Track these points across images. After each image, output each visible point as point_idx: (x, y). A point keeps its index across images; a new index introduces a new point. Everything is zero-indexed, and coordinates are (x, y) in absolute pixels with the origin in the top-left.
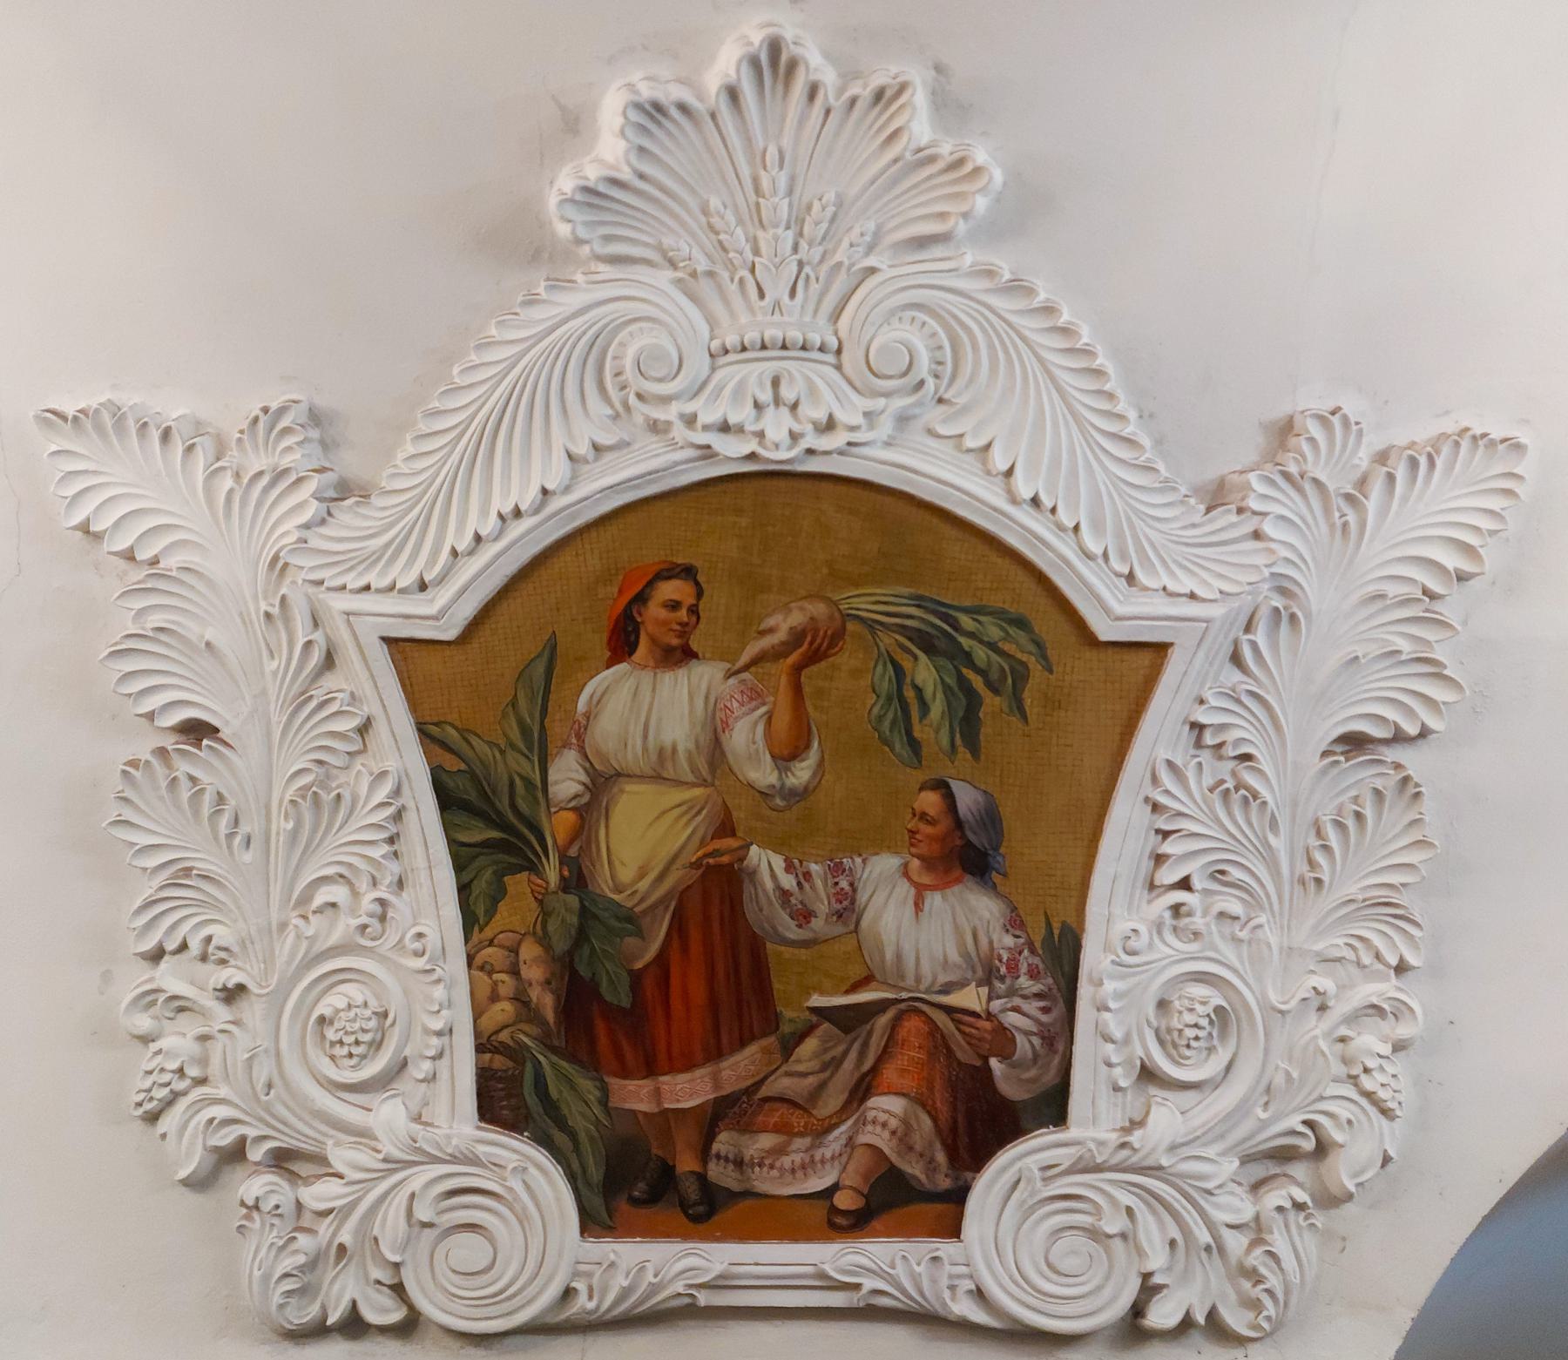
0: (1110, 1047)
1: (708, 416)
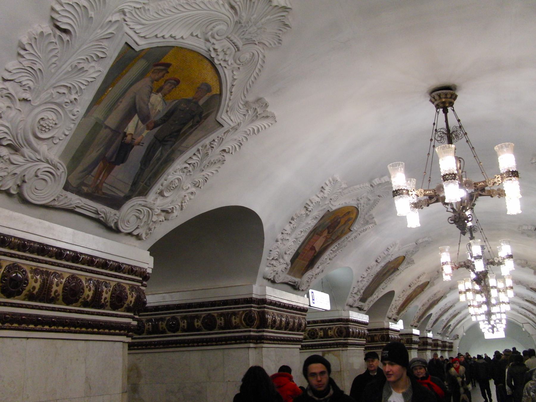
1: (216, 47)
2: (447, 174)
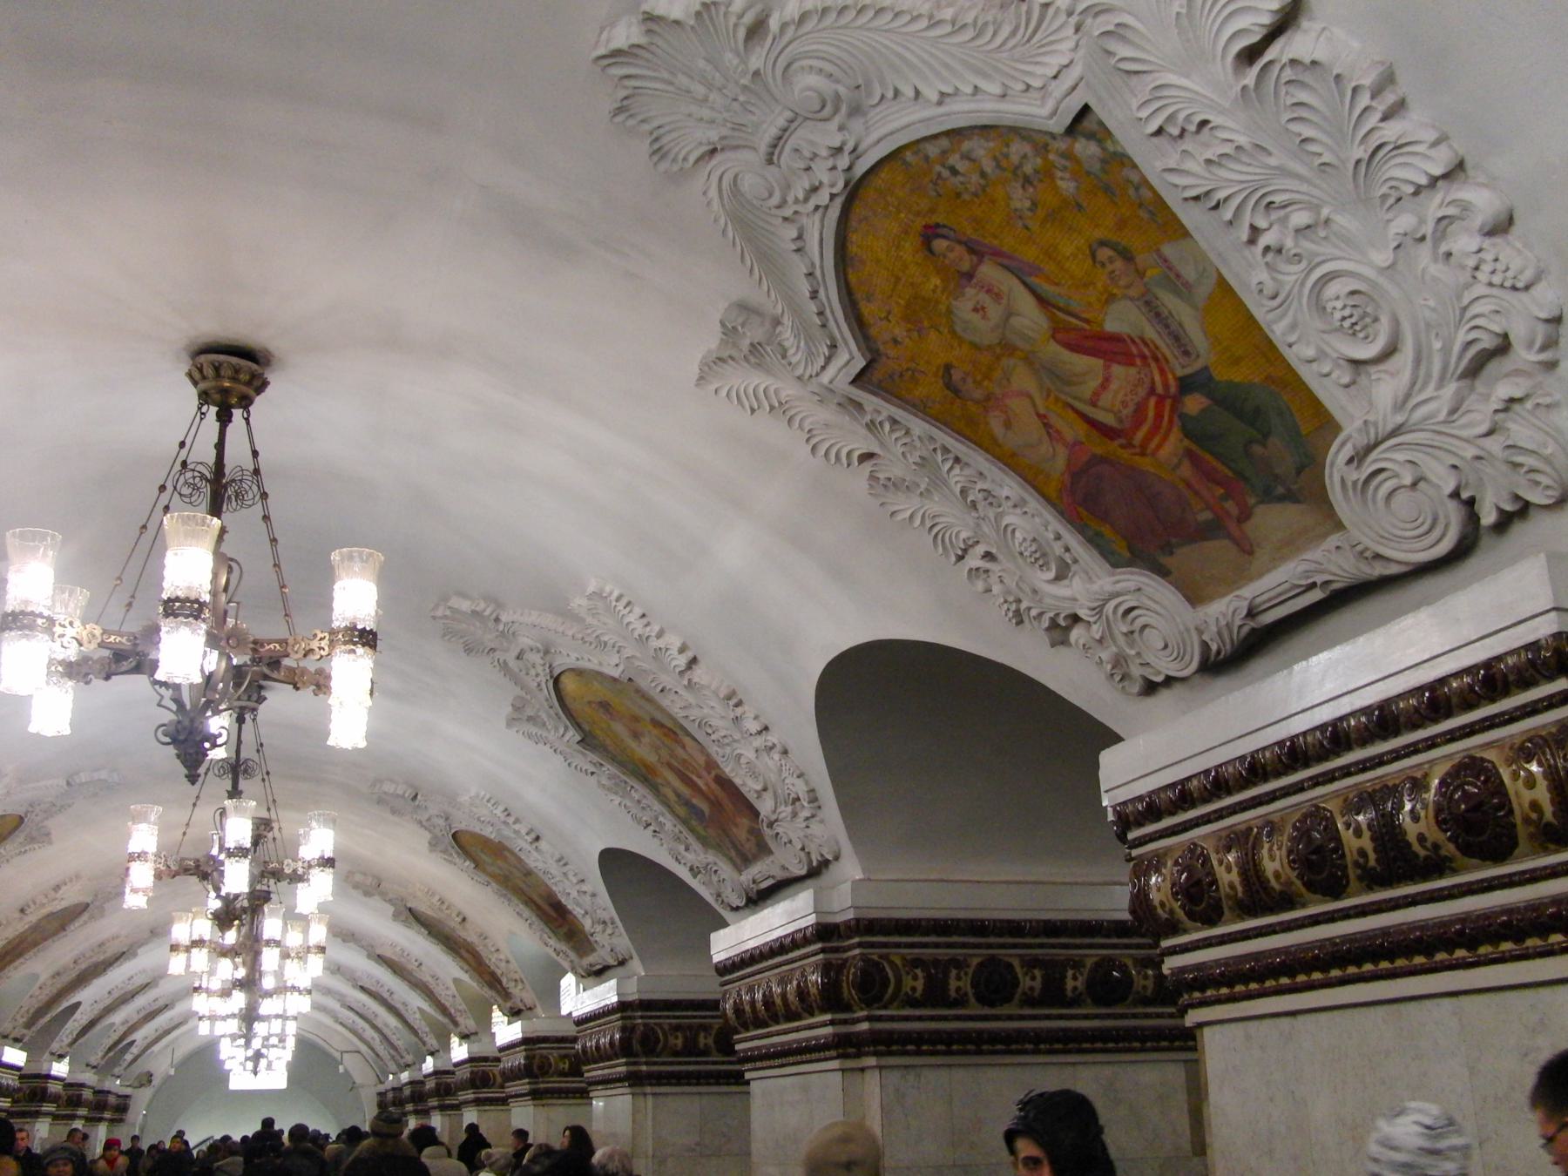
0: (1314, 365)
2: (177, 599)
